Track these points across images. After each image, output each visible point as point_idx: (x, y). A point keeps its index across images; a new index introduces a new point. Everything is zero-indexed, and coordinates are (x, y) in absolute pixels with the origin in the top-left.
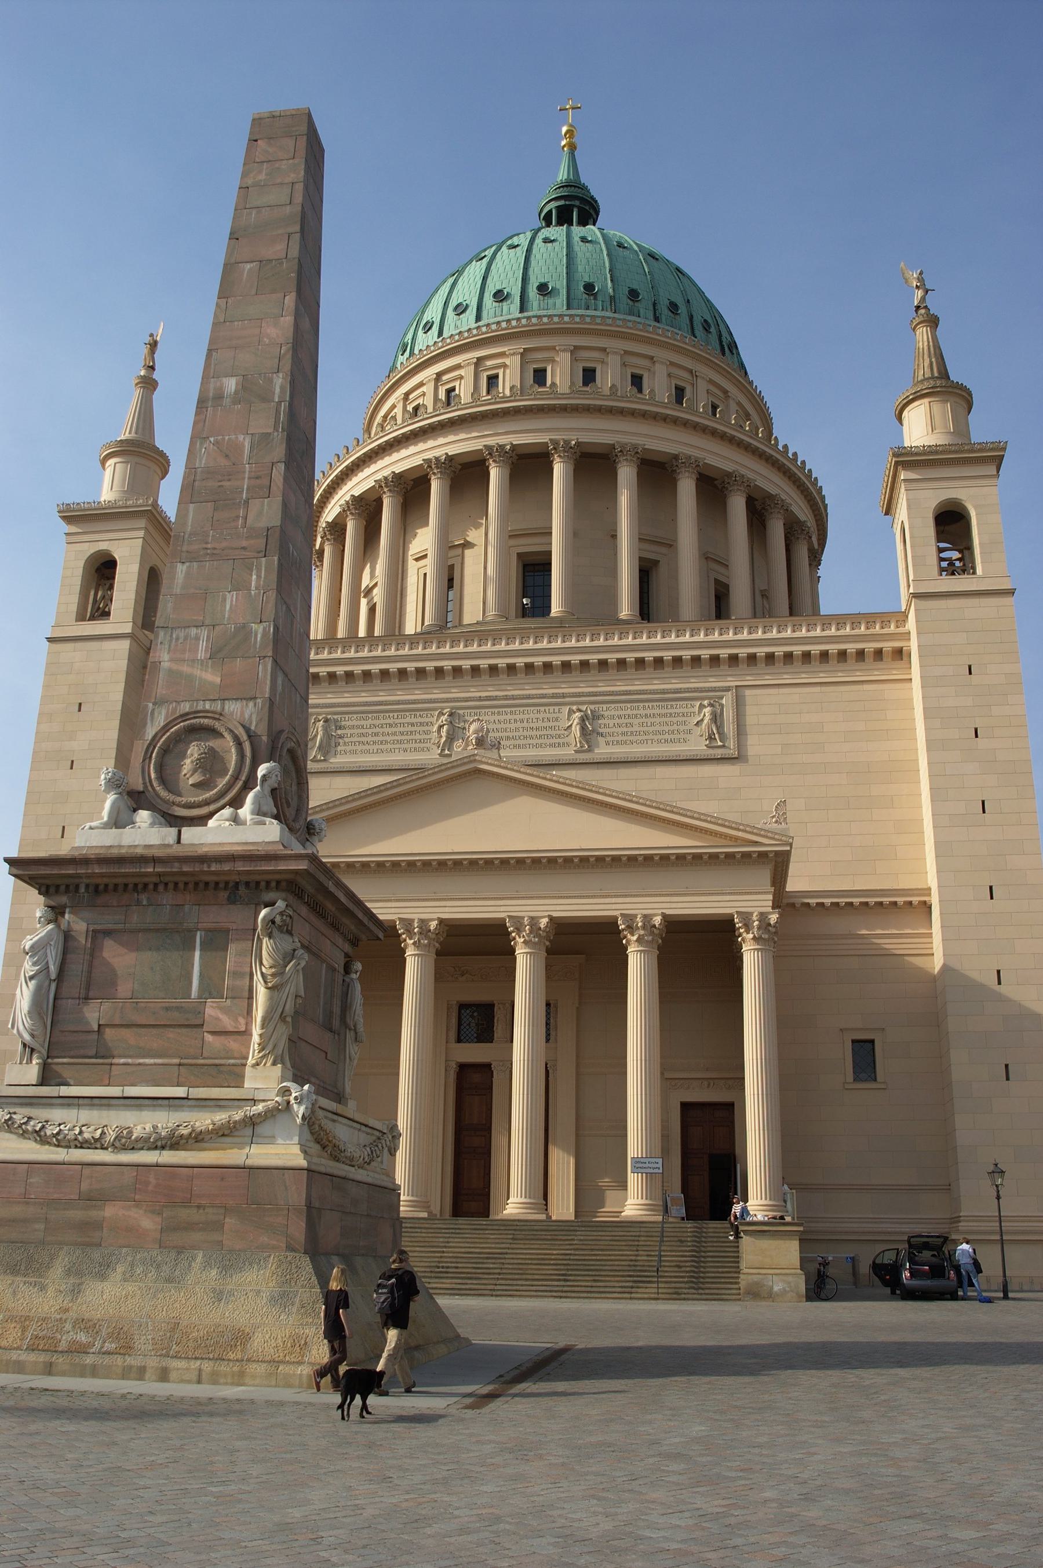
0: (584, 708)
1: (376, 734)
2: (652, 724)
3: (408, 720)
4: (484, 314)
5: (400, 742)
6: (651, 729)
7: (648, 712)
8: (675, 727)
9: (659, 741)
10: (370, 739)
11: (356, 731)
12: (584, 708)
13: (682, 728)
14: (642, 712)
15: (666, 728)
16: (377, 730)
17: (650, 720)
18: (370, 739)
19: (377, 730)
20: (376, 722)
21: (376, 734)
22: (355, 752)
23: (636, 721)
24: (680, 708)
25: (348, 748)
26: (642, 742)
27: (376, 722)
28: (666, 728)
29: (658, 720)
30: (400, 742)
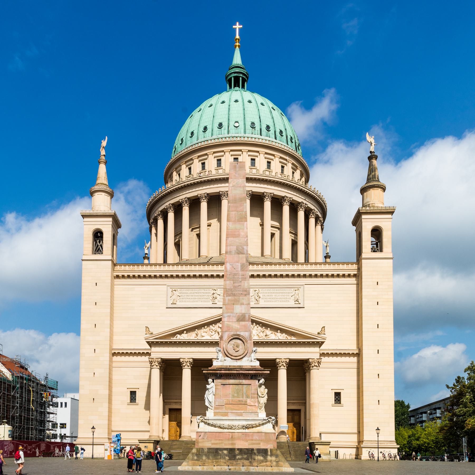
0: (257, 289)
1: (192, 296)
2: (279, 296)
3: (202, 291)
4: (214, 133)
5: (200, 298)
6: (278, 297)
7: (278, 292)
8: (286, 297)
9: (281, 301)
10: (190, 297)
11: (186, 295)
12: (257, 289)
13: (288, 297)
14: (276, 292)
15: (283, 297)
16: (192, 294)
17: (278, 294)
18: (190, 297)
19: (192, 294)
20: (192, 292)
21: (192, 296)
22: (186, 301)
23: (274, 295)
24: (287, 290)
25: (183, 300)
26: (275, 301)
27: (192, 292)
28: (283, 297)
29: (280, 294)
30: (200, 298)
